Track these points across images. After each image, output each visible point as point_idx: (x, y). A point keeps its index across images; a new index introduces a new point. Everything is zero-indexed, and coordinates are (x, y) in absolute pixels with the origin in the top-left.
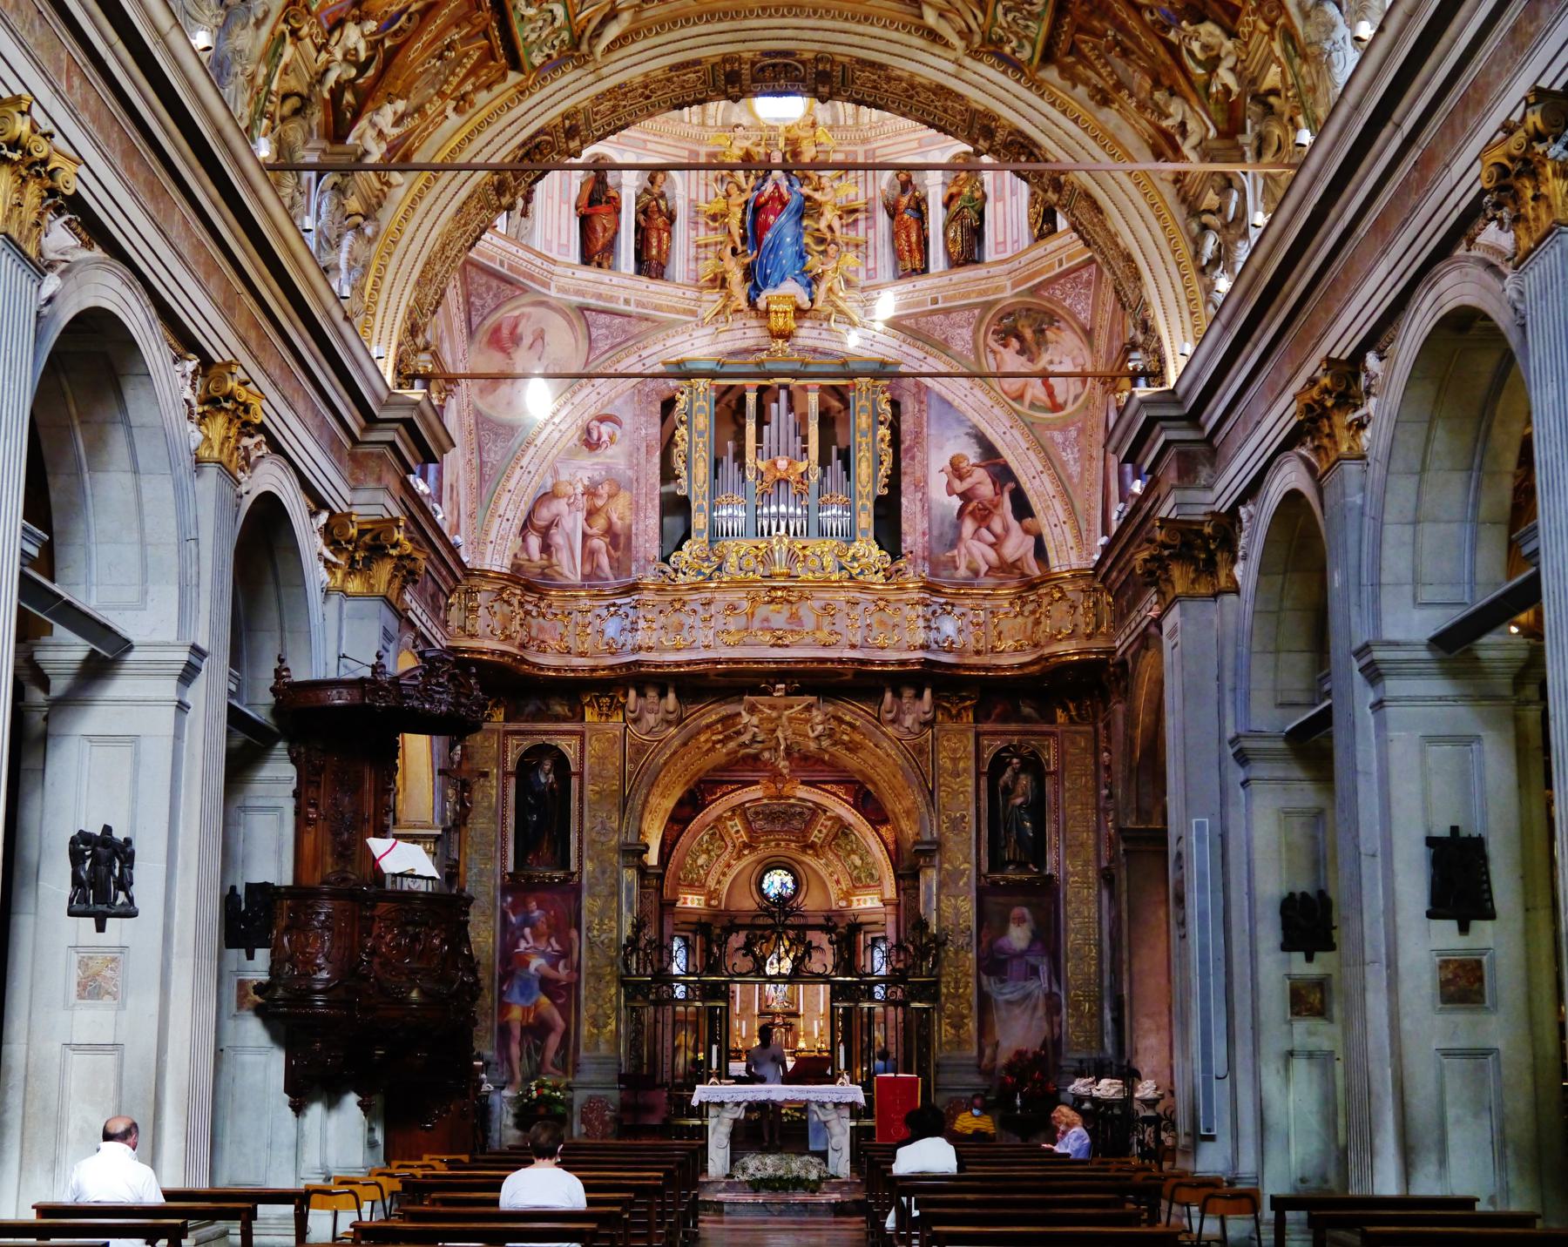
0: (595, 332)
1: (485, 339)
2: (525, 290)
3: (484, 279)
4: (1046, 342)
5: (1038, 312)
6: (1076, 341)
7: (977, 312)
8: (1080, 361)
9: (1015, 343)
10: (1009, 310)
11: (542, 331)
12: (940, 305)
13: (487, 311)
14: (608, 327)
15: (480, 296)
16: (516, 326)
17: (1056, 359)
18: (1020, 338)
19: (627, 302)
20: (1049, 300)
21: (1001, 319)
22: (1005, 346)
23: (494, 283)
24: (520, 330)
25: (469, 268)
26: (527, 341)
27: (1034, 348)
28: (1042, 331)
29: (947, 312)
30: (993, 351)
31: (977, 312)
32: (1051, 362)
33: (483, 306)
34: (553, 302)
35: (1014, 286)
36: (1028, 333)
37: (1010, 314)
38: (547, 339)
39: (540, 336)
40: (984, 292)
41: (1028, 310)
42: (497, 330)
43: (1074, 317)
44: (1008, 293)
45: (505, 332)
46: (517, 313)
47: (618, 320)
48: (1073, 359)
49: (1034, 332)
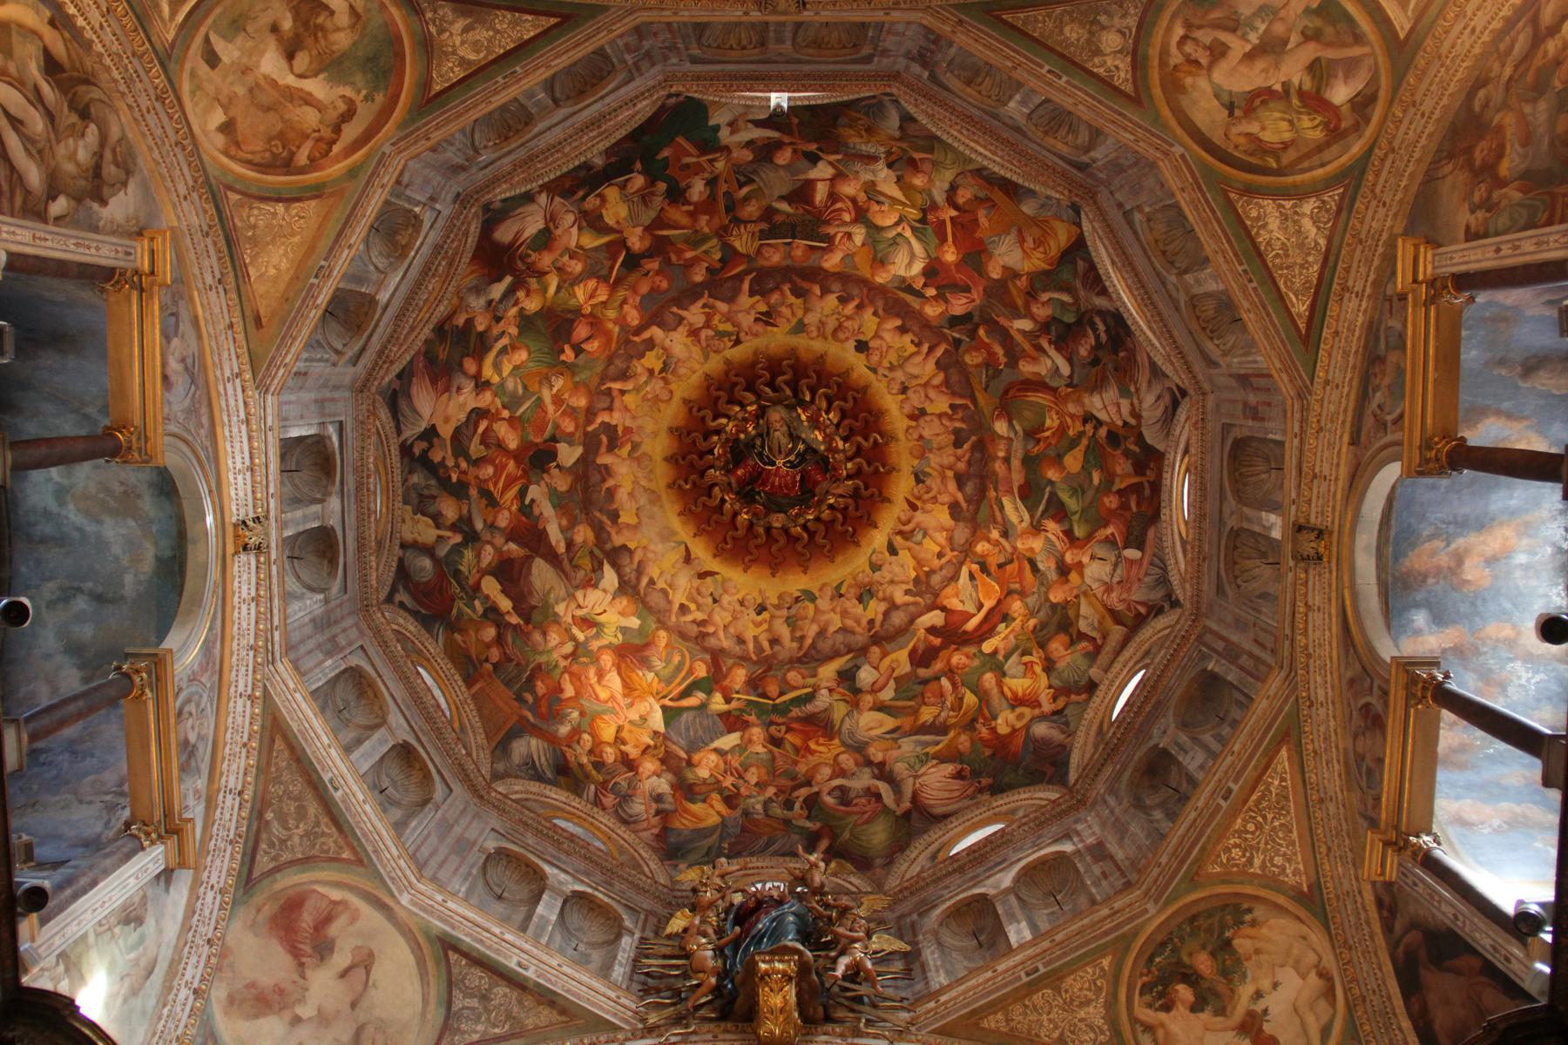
0: (459, 1002)
1: (268, 911)
2: (361, 860)
3: (298, 787)
4: (1239, 962)
5: (1210, 914)
6: (1291, 926)
7: (1106, 962)
8: (1311, 958)
9: (1184, 992)
10: (1159, 938)
11: (371, 955)
12: (1042, 970)
13: (286, 856)
14: (484, 998)
15: (282, 818)
16: (327, 920)
17: (1265, 984)
18: (1190, 977)
19: (520, 964)
20: (1224, 879)
21: (1151, 959)
22: (1167, 1008)
23: (313, 808)
24: (333, 930)
25: (279, 744)
26: (341, 959)
27: (1221, 987)
28: (1227, 944)
29: (1054, 979)
30: (1149, 1028)
31: (1106, 962)
32: (1258, 995)
33: (283, 842)
34: (402, 914)
35: (1156, 901)
36: (1203, 963)
37: (1163, 944)
38: (377, 973)
39: (365, 962)
40: (1117, 927)
41: (1194, 917)
42: (293, 905)
43: (1273, 883)
44: (1152, 911)
45: (307, 919)
46: (336, 895)
47: (502, 990)
48: (1296, 969)
49: (1213, 954)
